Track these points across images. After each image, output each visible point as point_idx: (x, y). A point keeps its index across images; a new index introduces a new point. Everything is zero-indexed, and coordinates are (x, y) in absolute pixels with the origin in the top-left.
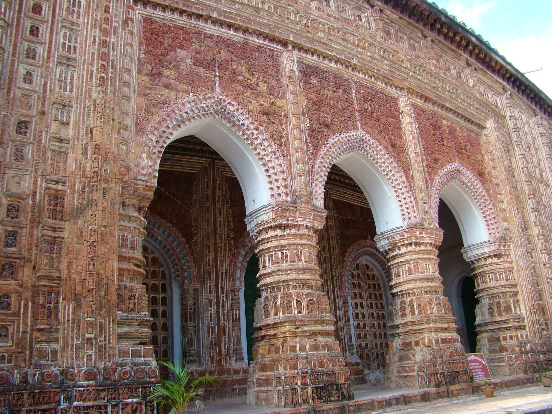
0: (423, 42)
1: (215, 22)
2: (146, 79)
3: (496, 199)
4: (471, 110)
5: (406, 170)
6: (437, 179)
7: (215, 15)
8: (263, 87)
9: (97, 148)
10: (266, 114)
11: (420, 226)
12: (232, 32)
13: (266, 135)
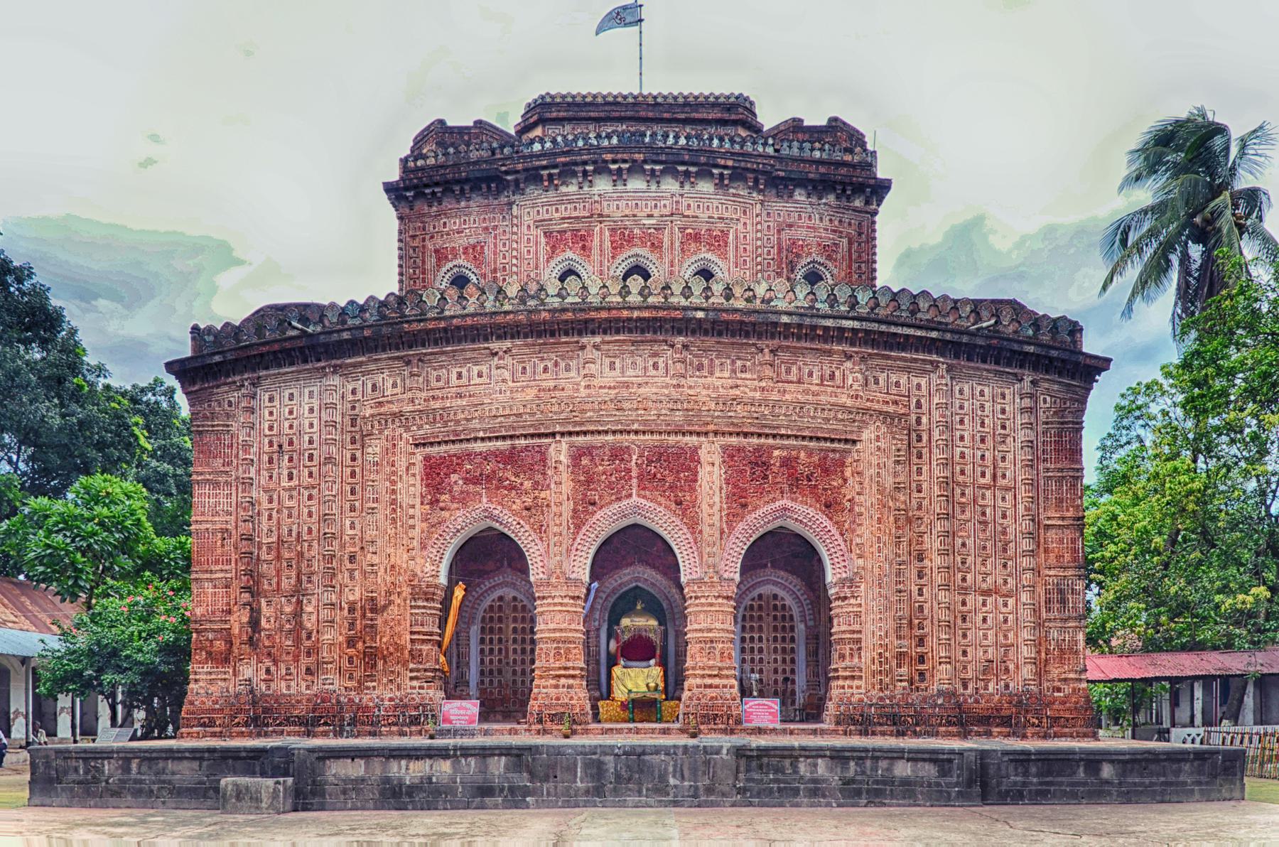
0: (759, 357)
1: (483, 439)
2: (428, 507)
3: (853, 531)
4: (833, 425)
5: (693, 525)
6: (741, 526)
7: (481, 434)
8: (528, 484)
9: (393, 566)
10: (528, 509)
11: (700, 582)
12: (499, 443)
13: (527, 527)
